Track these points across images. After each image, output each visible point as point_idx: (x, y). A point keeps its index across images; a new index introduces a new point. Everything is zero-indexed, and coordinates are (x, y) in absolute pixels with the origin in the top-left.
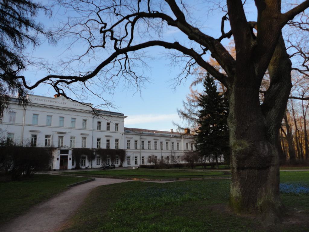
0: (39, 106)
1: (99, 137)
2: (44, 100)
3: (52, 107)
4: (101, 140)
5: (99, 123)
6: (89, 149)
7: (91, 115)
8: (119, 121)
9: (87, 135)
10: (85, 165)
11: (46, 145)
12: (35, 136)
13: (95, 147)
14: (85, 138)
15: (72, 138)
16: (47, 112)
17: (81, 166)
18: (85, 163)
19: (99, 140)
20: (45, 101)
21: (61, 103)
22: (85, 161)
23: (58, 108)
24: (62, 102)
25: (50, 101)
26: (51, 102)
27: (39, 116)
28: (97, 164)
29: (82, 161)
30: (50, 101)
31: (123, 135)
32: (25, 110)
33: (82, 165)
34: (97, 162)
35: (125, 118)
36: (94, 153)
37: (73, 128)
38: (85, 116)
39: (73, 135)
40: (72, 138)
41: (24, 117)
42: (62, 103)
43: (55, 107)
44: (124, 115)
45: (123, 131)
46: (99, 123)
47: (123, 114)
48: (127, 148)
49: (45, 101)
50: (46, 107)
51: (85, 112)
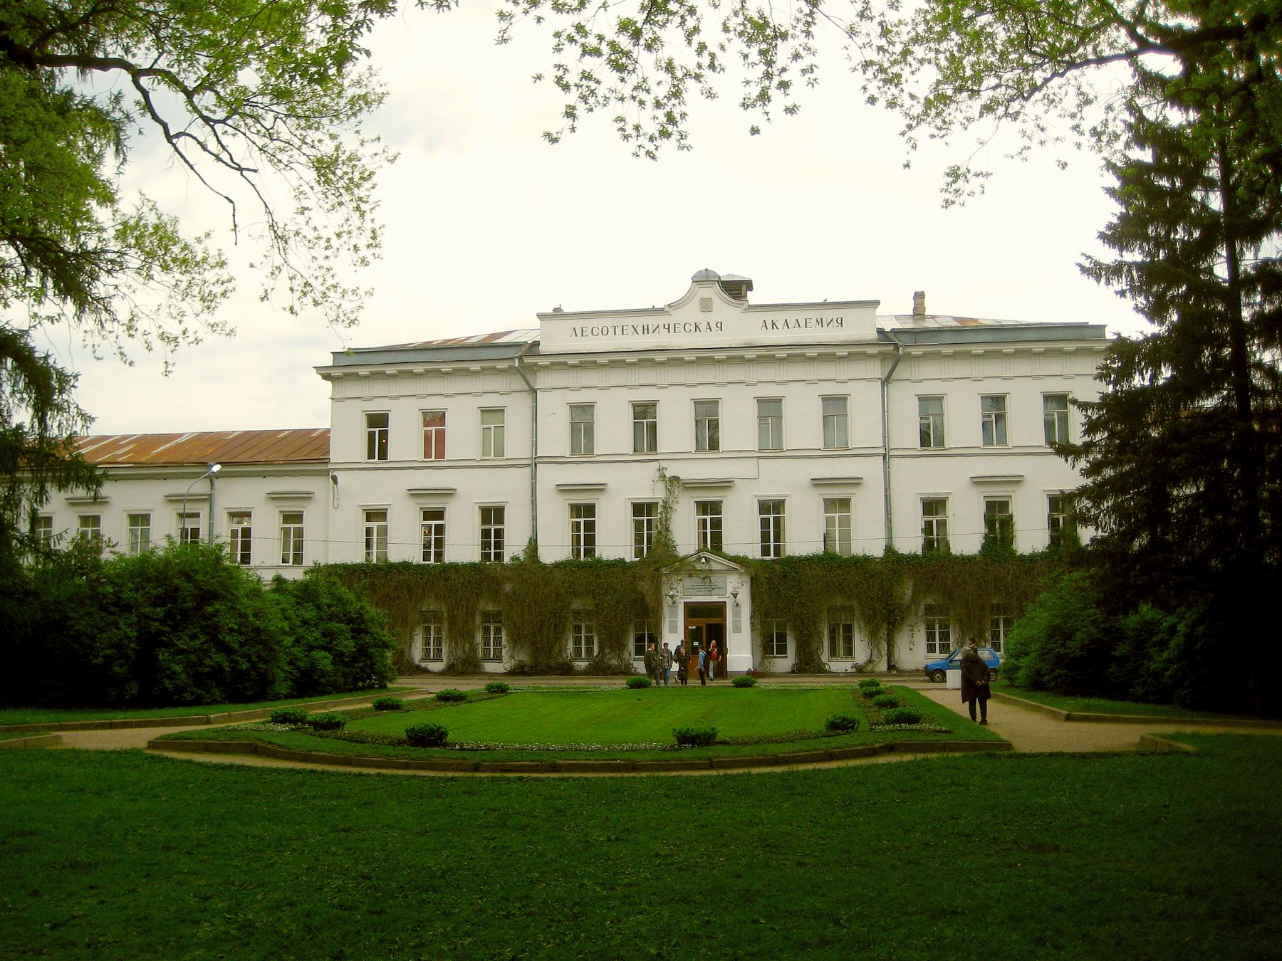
0: (587, 362)
1: (933, 490)
2: (611, 330)
3: (646, 360)
4: (950, 507)
5: (931, 403)
6: (863, 562)
7: (876, 370)
8: (1005, 379)
9: (855, 482)
10: (849, 652)
11: (639, 552)
12: (590, 510)
13: (910, 542)
14: (845, 504)
17: (825, 657)
18: (849, 640)
19: (933, 506)
20: (619, 330)
22: (848, 629)
23: (675, 359)
24: (702, 319)
25: (640, 330)
26: (646, 330)
27: (598, 412)
28: (931, 648)
30: (640, 330)
32: (535, 391)
33: (833, 653)
34: (930, 636)
38: (830, 379)
39: (772, 493)
42: (703, 327)
43: (660, 357)
46: (931, 403)
47: (1102, 328)
49: (619, 330)
50: (617, 361)
51: (827, 354)
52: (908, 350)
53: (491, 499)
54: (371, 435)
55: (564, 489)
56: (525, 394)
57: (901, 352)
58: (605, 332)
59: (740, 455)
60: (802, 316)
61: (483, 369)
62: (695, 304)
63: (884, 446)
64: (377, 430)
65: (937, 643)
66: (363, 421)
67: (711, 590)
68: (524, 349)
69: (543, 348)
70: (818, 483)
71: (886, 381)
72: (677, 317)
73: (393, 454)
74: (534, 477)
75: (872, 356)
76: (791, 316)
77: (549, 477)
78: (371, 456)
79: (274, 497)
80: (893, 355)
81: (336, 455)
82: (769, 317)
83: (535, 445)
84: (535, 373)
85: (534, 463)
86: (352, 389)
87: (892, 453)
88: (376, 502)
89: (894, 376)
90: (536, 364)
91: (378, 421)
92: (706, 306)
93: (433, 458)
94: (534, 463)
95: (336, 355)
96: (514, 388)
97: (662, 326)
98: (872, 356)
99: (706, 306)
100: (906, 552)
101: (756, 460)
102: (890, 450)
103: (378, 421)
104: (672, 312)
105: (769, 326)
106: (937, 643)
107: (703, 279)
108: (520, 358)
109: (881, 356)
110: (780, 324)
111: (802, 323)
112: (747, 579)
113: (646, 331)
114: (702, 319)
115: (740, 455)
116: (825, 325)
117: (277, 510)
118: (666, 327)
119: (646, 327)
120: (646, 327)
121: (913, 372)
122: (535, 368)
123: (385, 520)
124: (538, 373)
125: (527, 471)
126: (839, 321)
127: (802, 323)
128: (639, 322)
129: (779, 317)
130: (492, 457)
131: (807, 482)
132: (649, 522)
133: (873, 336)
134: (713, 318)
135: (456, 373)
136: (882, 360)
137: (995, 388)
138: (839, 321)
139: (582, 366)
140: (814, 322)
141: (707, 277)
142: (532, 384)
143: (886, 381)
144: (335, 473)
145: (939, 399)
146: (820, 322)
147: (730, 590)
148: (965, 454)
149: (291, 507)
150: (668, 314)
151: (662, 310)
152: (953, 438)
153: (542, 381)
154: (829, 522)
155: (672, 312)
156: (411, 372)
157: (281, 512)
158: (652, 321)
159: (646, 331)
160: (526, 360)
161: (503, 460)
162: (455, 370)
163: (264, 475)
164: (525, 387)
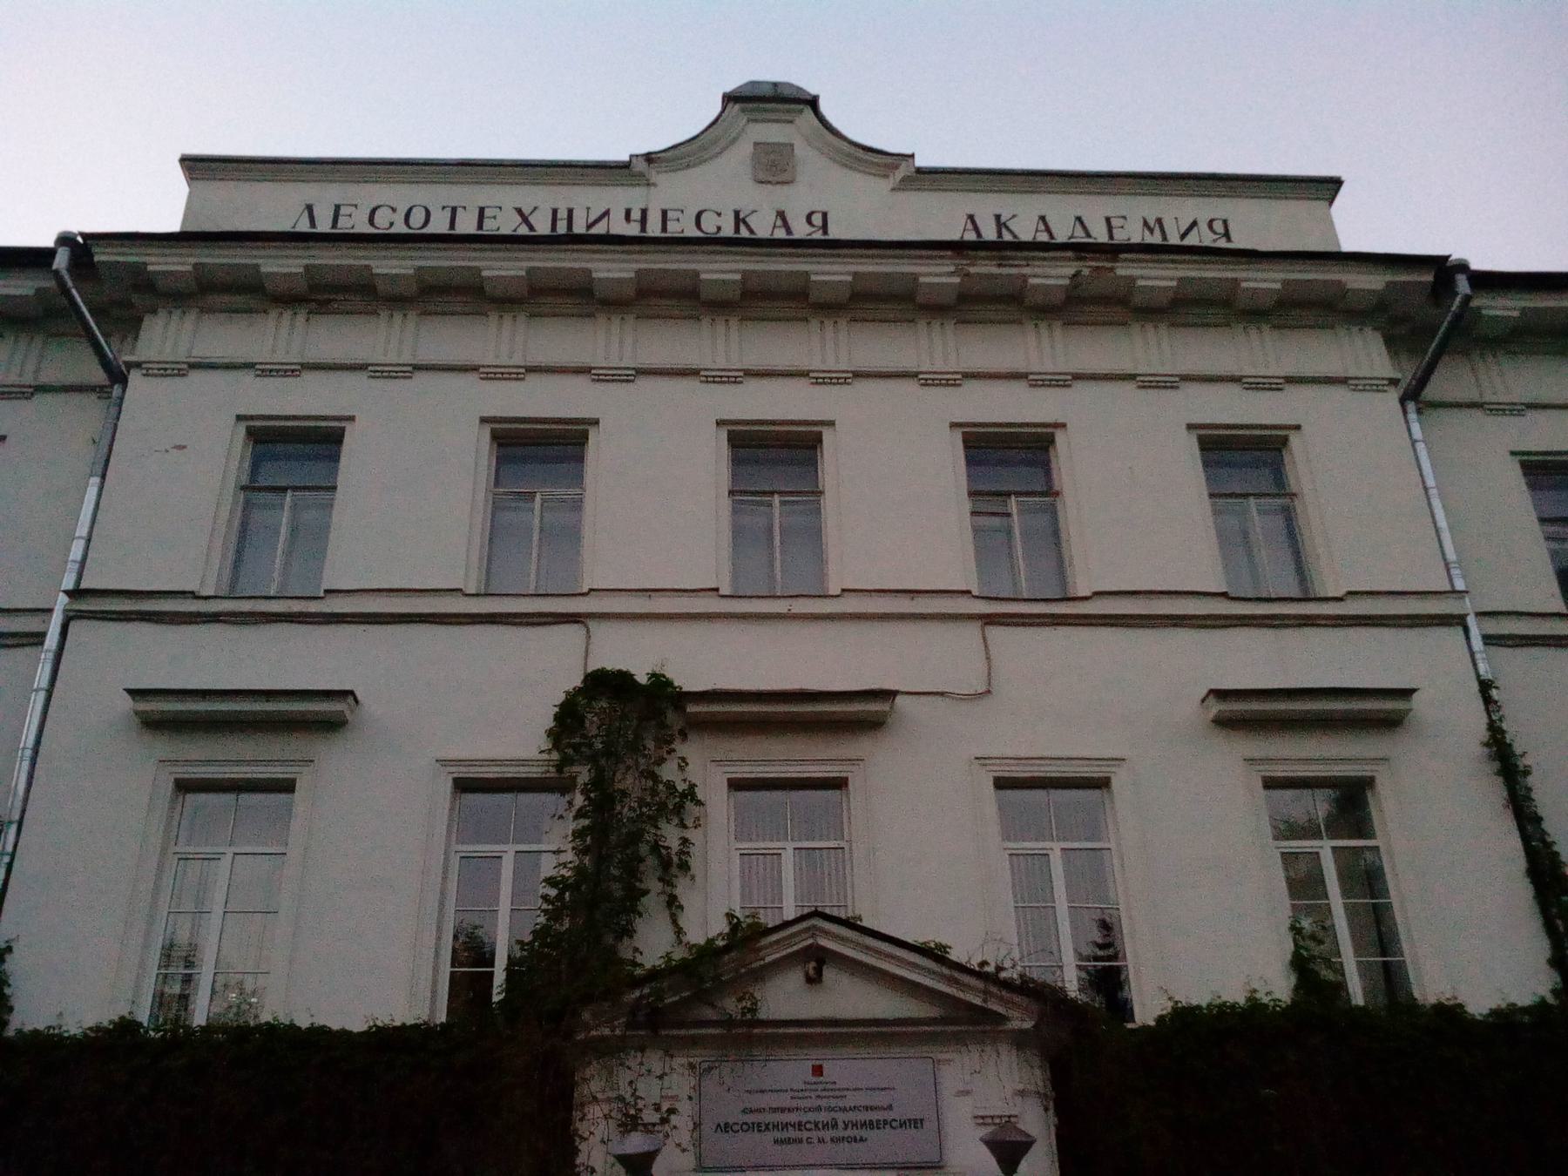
41: (95, 480)
96: (49, 376)
101: (972, 631)
104: (654, 177)
118: (636, 215)
150: (642, 180)
151: (625, 166)
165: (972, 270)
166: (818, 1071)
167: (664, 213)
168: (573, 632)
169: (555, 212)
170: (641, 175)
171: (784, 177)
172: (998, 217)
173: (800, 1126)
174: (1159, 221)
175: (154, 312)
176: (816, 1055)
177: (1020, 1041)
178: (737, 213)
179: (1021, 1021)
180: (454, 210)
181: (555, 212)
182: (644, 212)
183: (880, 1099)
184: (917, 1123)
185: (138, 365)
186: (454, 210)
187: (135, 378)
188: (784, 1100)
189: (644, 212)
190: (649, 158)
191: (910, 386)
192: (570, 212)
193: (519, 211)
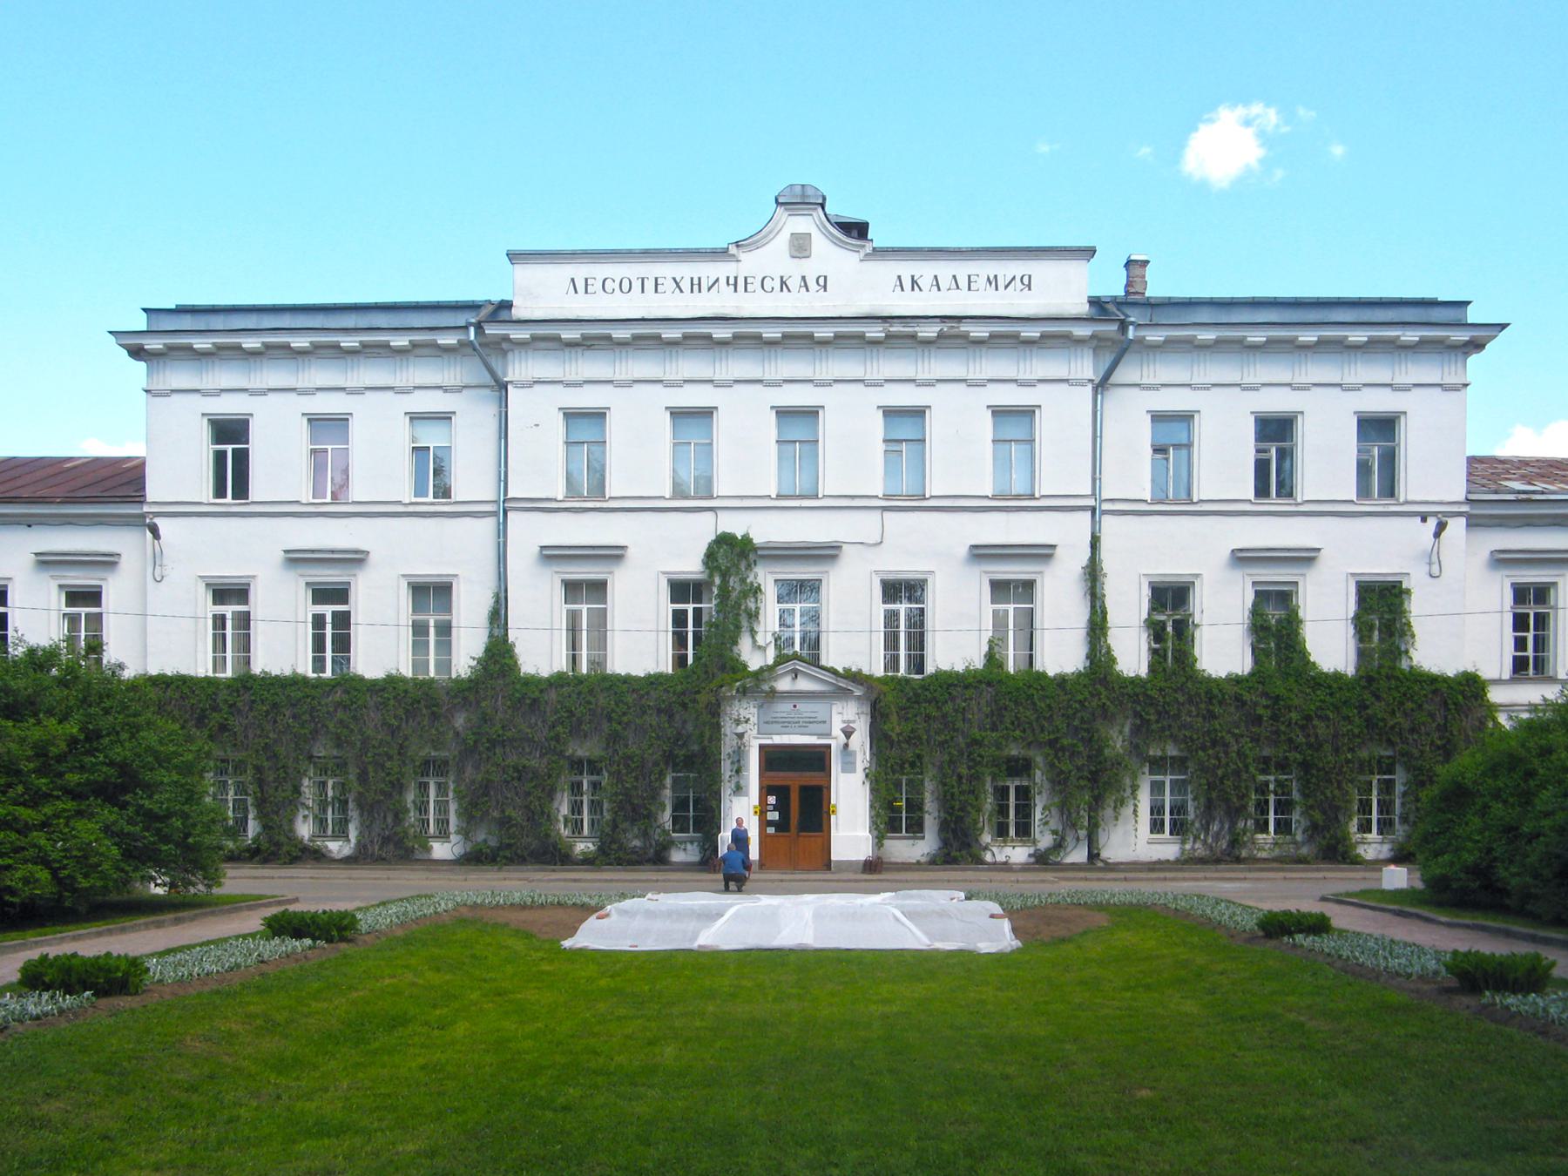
2: (637, 285)
7: (1085, 367)
9: (1043, 553)
15: (894, 589)
16: (569, 385)
20: (650, 285)
21: (783, 283)
24: (794, 269)
25: (686, 285)
26: (696, 285)
27: (612, 421)
29: (1002, 793)
30: (686, 285)
31: (1441, 527)
32: (502, 387)
35: (1477, 345)
36: (1117, 739)
37: (916, 502)
39: (903, 566)
40: (894, 589)
42: (794, 283)
44: (1473, 315)
45: (1454, 488)
48: (1507, 673)
49: (650, 285)
52: (1141, 333)
53: (429, 569)
54: (220, 458)
55: (551, 555)
56: (487, 392)
57: (1131, 333)
58: (625, 287)
59: (851, 504)
60: (963, 269)
61: (414, 345)
62: (781, 243)
63: (1094, 494)
64: (229, 448)
65: (1375, 816)
66: (205, 432)
67: (803, 725)
68: (484, 313)
69: (518, 313)
70: (981, 554)
71: (1102, 385)
72: (750, 264)
73: (257, 490)
74: (502, 532)
75: (1080, 342)
76: (945, 270)
77: (528, 533)
78: (220, 491)
79: (46, 562)
80: (1114, 342)
81: (157, 489)
82: (907, 269)
83: (503, 480)
84: (504, 353)
85: (503, 509)
86: (179, 376)
87: (1105, 506)
88: (229, 570)
89: (1113, 379)
90: (506, 338)
91: (230, 431)
92: (800, 246)
93: (329, 499)
94: (503, 509)
95: (154, 316)
97: (723, 281)
98: (1080, 342)
99: (800, 246)
100: (1222, 673)
102: (1102, 501)
103: (230, 431)
104: (742, 256)
105: (907, 284)
106: (1375, 816)
107: (800, 200)
108: (479, 327)
109: (1095, 343)
110: (925, 282)
111: (963, 283)
112: (867, 709)
113: (696, 287)
114: (794, 269)
115: (851, 504)
116: (1001, 284)
117: (54, 585)
118: (732, 281)
119: (696, 281)
120: (696, 281)
121: (1145, 374)
122: (503, 347)
123: (246, 602)
124: (510, 355)
125: (487, 526)
126: (1026, 280)
127: (963, 283)
128: (685, 271)
129: (925, 270)
130: (430, 498)
131: (963, 551)
132: (698, 612)
133: (1083, 309)
134: (811, 268)
135: (365, 351)
136: (1095, 350)
137: (1276, 402)
138: (1026, 280)
139: (586, 344)
140: (982, 281)
141: (803, 195)
142: (500, 373)
143: (1102, 385)
144: (157, 521)
145: (1186, 418)
146: (993, 281)
147: (837, 730)
148: (1225, 511)
149: (81, 579)
151: (725, 251)
152: (1206, 487)
153: (518, 369)
154: (999, 621)
155: (742, 256)
156: (286, 347)
157: (61, 586)
158: (708, 271)
159: (696, 287)
160: (491, 330)
161: (450, 504)
162: (364, 345)
163: (29, 522)
164: (488, 379)
165: (891, 329)
166: (795, 706)
167: (746, 279)
168: (710, 515)
169: (692, 279)
170: (734, 255)
171: (807, 254)
172: (913, 277)
173: (789, 722)
174: (996, 276)
175: (512, 350)
176: (795, 702)
177: (859, 698)
178: (782, 278)
179: (858, 693)
180: (643, 280)
181: (692, 279)
182: (736, 278)
183: (813, 715)
184: (825, 722)
185: (511, 382)
186: (643, 280)
187: (509, 387)
188: (784, 715)
189: (736, 278)
190: (737, 244)
191: (860, 386)
192: (699, 279)
193: (674, 279)
